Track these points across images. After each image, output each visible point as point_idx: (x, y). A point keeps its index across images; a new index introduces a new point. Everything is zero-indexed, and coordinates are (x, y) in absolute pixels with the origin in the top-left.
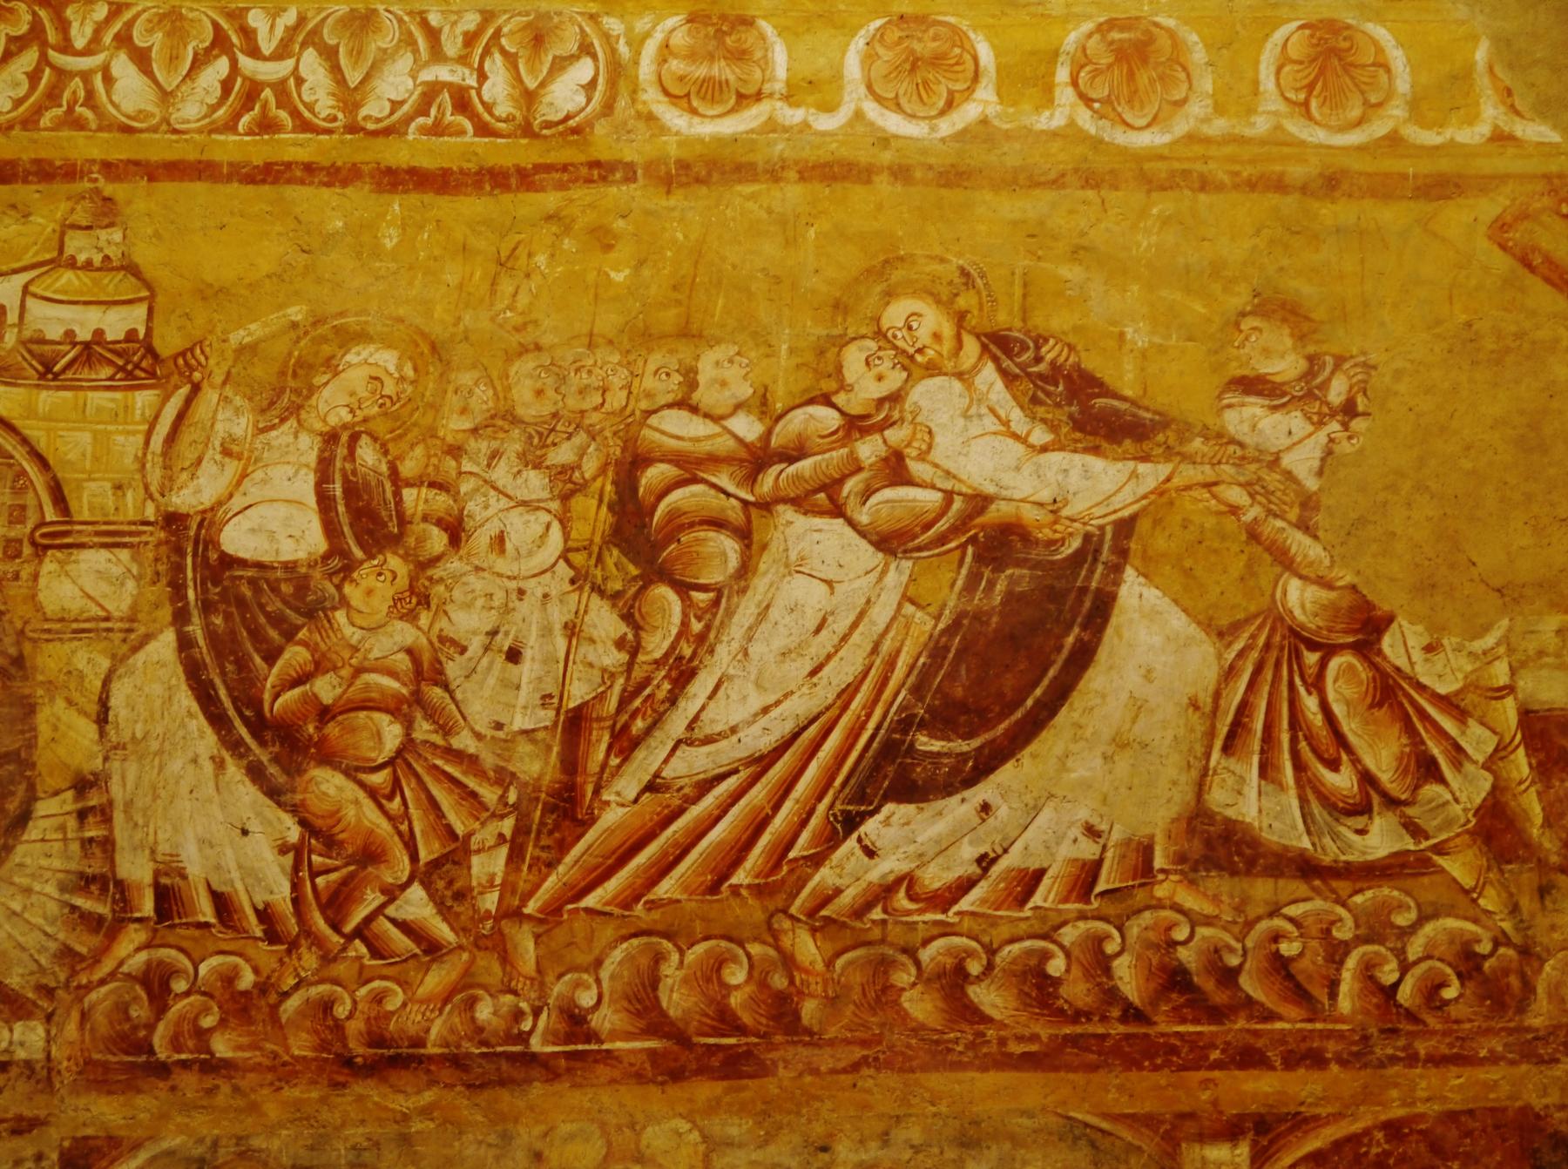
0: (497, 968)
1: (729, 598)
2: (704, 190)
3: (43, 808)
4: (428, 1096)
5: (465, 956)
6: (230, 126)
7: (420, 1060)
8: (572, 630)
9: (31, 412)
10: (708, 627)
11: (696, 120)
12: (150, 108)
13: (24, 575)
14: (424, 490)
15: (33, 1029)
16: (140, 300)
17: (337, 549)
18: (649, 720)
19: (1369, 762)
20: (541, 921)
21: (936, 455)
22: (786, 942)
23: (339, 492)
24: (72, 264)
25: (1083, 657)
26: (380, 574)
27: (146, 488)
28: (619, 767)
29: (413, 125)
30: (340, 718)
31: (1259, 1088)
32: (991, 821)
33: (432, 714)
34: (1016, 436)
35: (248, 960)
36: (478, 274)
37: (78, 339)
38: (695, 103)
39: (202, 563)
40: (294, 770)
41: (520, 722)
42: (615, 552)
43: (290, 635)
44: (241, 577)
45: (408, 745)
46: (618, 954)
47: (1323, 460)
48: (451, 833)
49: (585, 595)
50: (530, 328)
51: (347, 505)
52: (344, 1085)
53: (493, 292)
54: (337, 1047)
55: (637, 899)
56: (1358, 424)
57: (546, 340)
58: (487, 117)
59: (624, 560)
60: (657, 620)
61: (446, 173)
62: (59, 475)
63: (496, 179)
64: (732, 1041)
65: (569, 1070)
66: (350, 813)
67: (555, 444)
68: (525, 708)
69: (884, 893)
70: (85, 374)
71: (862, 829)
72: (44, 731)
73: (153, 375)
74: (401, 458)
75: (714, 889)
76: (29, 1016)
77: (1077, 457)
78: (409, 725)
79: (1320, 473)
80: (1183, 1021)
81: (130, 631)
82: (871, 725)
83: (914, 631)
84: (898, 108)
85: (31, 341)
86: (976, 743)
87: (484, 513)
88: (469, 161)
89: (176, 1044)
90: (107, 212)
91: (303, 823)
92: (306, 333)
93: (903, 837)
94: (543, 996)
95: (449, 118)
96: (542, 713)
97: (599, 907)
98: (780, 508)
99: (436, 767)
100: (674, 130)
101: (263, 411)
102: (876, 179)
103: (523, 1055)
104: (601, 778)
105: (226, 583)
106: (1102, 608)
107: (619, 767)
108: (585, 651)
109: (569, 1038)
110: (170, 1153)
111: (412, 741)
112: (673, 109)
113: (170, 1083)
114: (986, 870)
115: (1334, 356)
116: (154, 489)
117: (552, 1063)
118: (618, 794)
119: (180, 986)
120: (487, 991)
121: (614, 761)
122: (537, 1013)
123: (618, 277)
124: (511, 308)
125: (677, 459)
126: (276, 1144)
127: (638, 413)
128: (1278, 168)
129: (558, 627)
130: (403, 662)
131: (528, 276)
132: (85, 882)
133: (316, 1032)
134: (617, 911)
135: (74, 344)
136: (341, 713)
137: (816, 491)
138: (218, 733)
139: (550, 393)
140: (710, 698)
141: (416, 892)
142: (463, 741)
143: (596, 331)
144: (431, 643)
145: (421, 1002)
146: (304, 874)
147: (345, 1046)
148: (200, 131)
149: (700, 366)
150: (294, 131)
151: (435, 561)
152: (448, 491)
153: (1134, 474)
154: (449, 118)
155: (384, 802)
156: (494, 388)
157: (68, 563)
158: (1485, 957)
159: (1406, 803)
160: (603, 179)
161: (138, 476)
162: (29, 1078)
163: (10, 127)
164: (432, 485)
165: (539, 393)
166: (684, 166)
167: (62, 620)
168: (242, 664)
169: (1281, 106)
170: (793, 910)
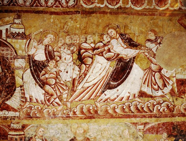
3: (17, 89)
8: (73, 69)
9: (12, 42)
10: (88, 69)
11: (87, 6)
13: (13, 62)
17: (47, 59)
19: (159, 85)
21: (114, 49)
22: (96, 104)
23: (47, 53)
24: (15, 23)
25: (129, 73)
27: (26, 52)
28: (79, 85)
29: (54, 6)
31: (144, 120)
32: (118, 92)
34: (123, 47)
39: (32, 61)
41: (68, 80)
42: (78, 60)
43: (42, 69)
45: (56, 82)
47: (157, 49)
51: (48, 54)
56: (161, 45)
60: (83, 68)
64: (91, 115)
66: (50, 90)
69: (107, 100)
70: (18, 37)
71: (105, 93)
74: (54, 48)
75: (89, 99)
76: (17, 112)
77: (129, 49)
78: (56, 80)
79: (156, 51)
80: (138, 113)
81: (25, 69)
82: (106, 81)
83: (111, 70)
84: (111, 5)
85: (11, 33)
86: (117, 83)
87: (64, 56)
91: (45, 91)
93: (110, 94)
95: (58, 5)
98: (96, 55)
99: (59, 85)
102: (108, 14)
105: (35, 63)
106: (132, 67)
107: (79, 85)
108: (75, 72)
109: (74, 115)
114: (118, 97)
115: (159, 37)
119: (33, 109)
121: (78, 85)
122: (70, 112)
123: (78, 26)
125: (85, 49)
128: (154, 13)
129: (72, 69)
130: (55, 73)
132: (22, 97)
135: (16, 34)
137: (100, 53)
138: (35, 81)
139: (70, 41)
141: (57, 99)
142: (62, 82)
143: (76, 33)
153: (135, 51)
158: (170, 106)
159: (162, 89)
164: (58, 52)
165: (69, 41)
167: (17, 67)
168: (38, 73)
169: (155, 5)
170: (97, 101)
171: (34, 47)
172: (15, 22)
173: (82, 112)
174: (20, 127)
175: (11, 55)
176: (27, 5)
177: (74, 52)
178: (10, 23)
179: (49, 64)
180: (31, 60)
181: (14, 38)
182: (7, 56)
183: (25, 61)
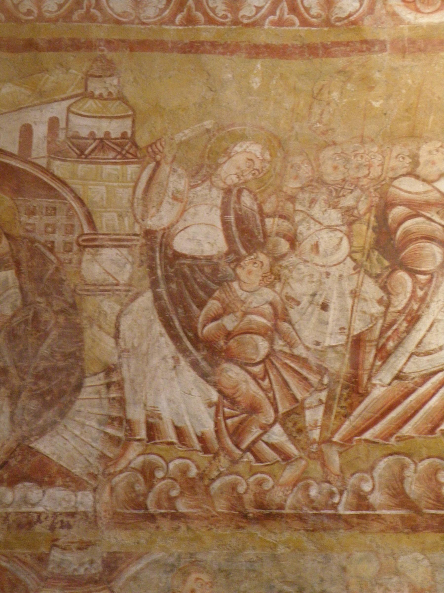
0: (319, 468)
1: (437, 278)
2: (423, 56)
3: (88, 382)
4: (287, 535)
5: (304, 462)
6: (172, 21)
7: (281, 516)
8: (355, 294)
10: (426, 294)
11: (419, 15)
12: (130, 10)
13: (74, 261)
14: (276, 219)
15: (87, 496)
16: (128, 116)
17: (232, 250)
18: (396, 342)
20: (342, 445)
24: (92, 96)
26: (255, 263)
27: (135, 216)
29: (267, 21)
30: (236, 338)
33: (284, 336)
35: (193, 462)
36: (302, 103)
37: (97, 137)
38: (419, 5)
40: (214, 365)
41: (329, 341)
42: (376, 253)
43: (210, 294)
44: (184, 264)
45: (271, 353)
46: (382, 464)
48: (295, 399)
49: (361, 276)
50: (330, 133)
51: (237, 227)
52: (243, 528)
53: (310, 113)
54: (239, 508)
55: (391, 435)
57: (339, 139)
58: (306, 15)
59: (381, 257)
60: (400, 289)
61: (285, 47)
62: (90, 209)
63: (311, 50)
65: (358, 524)
66: (243, 387)
67: (344, 196)
68: (331, 334)
70: (101, 155)
72: (88, 342)
73: (135, 156)
74: (263, 202)
76: (85, 489)
78: (272, 342)
81: (129, 291)
85: (73, 137)
88: (296, 40)
89: (159, 506)
90: (110, 69)
91: (220, 392)
92: (214, 135)
94: (344, 484)
95: (286, 16)
96: (340, 337)
97: (372, 439)
99: (286, 364)
100: (407, 21)
101: (193, 177)
103: (335, 515)
104: (371, 372)
105: (177, 267)
107: (381, 366)
108: (362, 305)
109: (358, 508)
110: (157, 561)
111: (273, 350)
112: (407, 9)
113: (156, 525)
116: (138, 217)
117: (349, 520)
118: (380, 380)
119: (159, 474)
120: (315, 481)
121: (378, 363)
122: (341, 493)
123: (376, 105)
124: (320, 121)
125: (408, 204)
126: (209, 558)
127: (387, 179)
129: (347, 292)
130: (268, 309)
131: (328, 104)
133: (229, 500)
134: (381, 441)
135: (95, 139)
136: (237, 335)
138: (175, 344)
139: (341, 168)
140: (428, 331)
141: (277, 428)
142: (300, 351)
144: (282, 299)
145: (281, 485)
146: (221, 418)
147: (244, 507)
148: (155, 23)
149: (421, 153)
150: (205, 24)
151: (283, 256)
152: (288, 220)
154: (286, 16)
155: (260, 381)
156: (312, 165)
157: (97, 255)
160: (369, 50)
161: (130, 210)
162: (85, 520)
163: (57, 20)
164: (281, 217)
165: (335, 168)
166: (412, 42)
167: (94, 285)
168: (187, 310)
171: (175, 198)
172: (90, 89)
173: (400, 497)
174: (95, 565)
175: (70, 229)
176: (149, 18)
177: (358, 219)
178: (69, 93)
179: (239, 271)
180: (158, 255)
181: (85, 158)
182: (51, 238)
183: (130, 259)
